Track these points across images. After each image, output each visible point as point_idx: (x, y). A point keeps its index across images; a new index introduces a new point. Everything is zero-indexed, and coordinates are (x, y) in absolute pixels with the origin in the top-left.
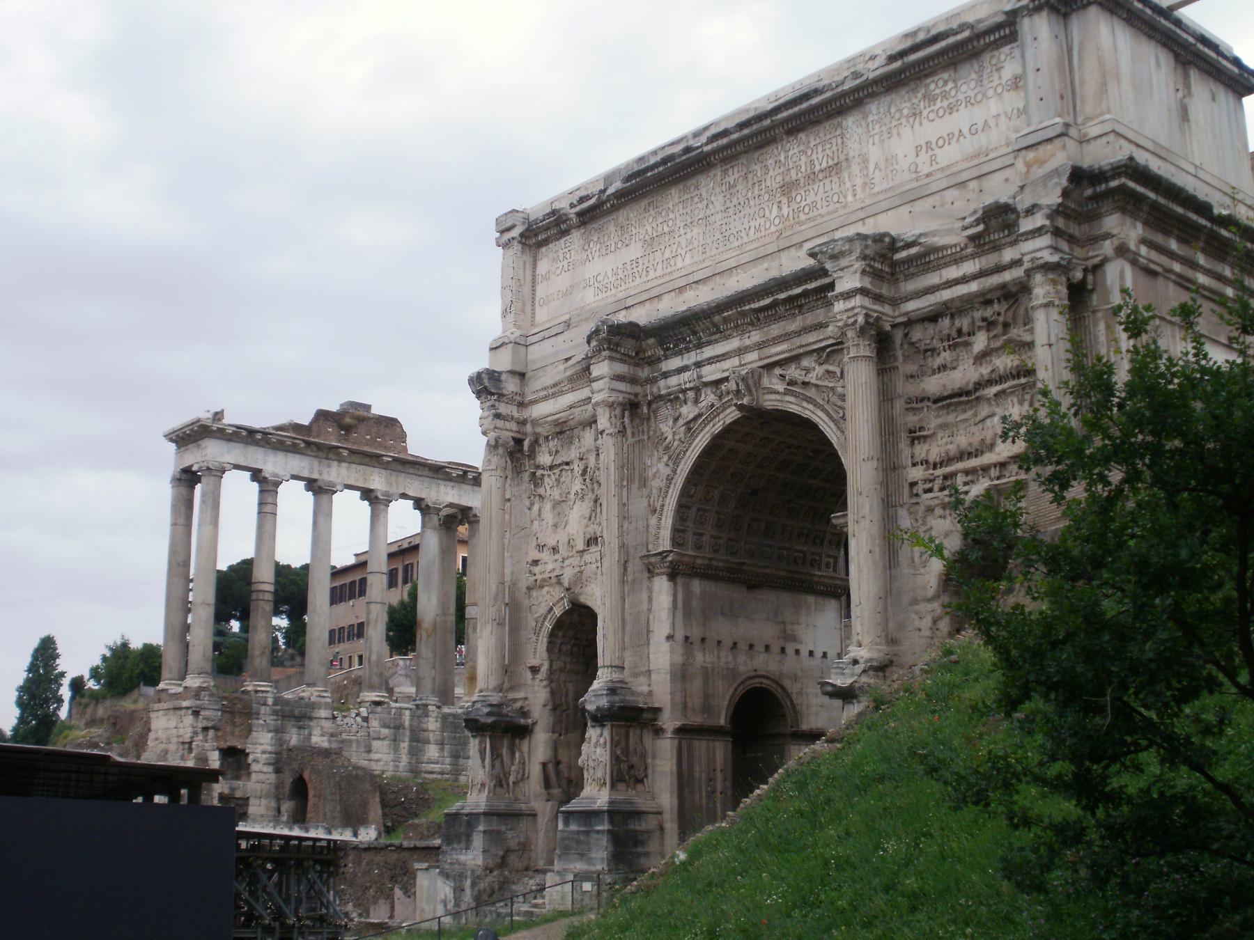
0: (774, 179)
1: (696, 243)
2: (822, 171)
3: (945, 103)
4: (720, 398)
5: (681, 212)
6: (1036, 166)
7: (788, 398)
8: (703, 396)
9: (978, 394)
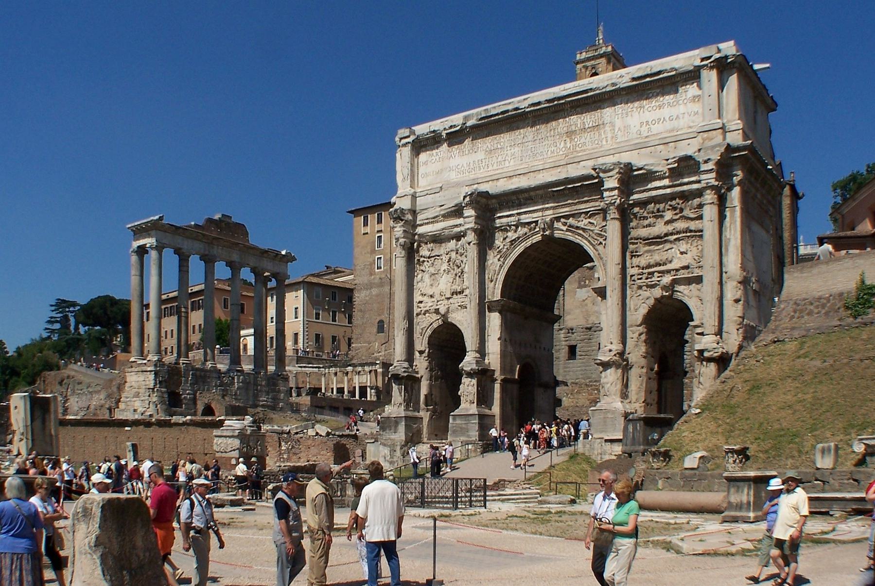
1: (517, 155)
2: (589, 128)
4: (530, 230)
5: (508, 139)
6: (707, 141)
7: (567, 233)
9: (666, 238)
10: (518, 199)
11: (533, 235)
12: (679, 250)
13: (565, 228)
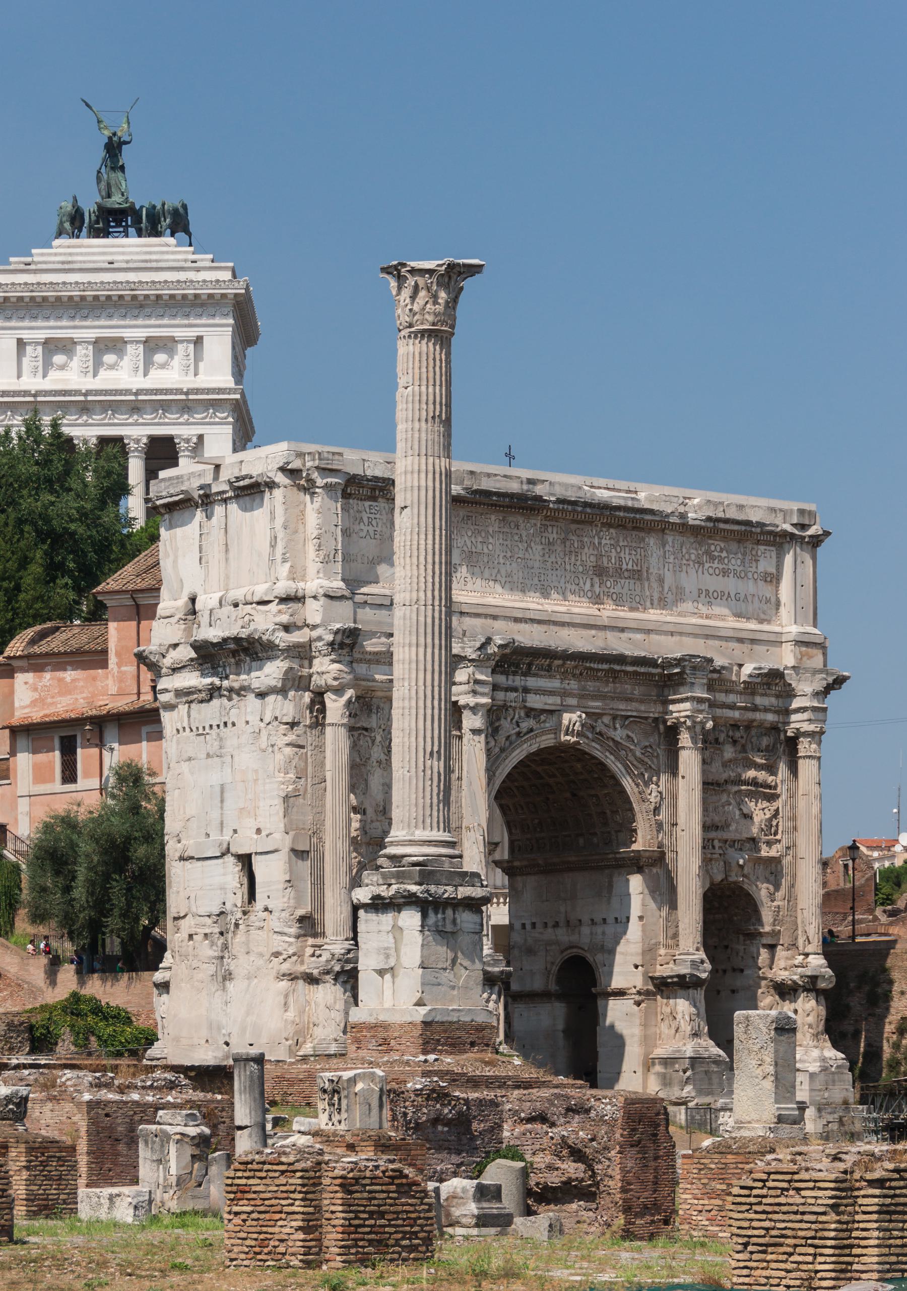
0: (588, 557)
1: (515, 578)
3: (721, 566)
5: (501, 541)
7: (594, 744)
8: (517, 716)
10: (530, 665)
11: (543, 733)
12: (741, 810)
13: (590, 735)
